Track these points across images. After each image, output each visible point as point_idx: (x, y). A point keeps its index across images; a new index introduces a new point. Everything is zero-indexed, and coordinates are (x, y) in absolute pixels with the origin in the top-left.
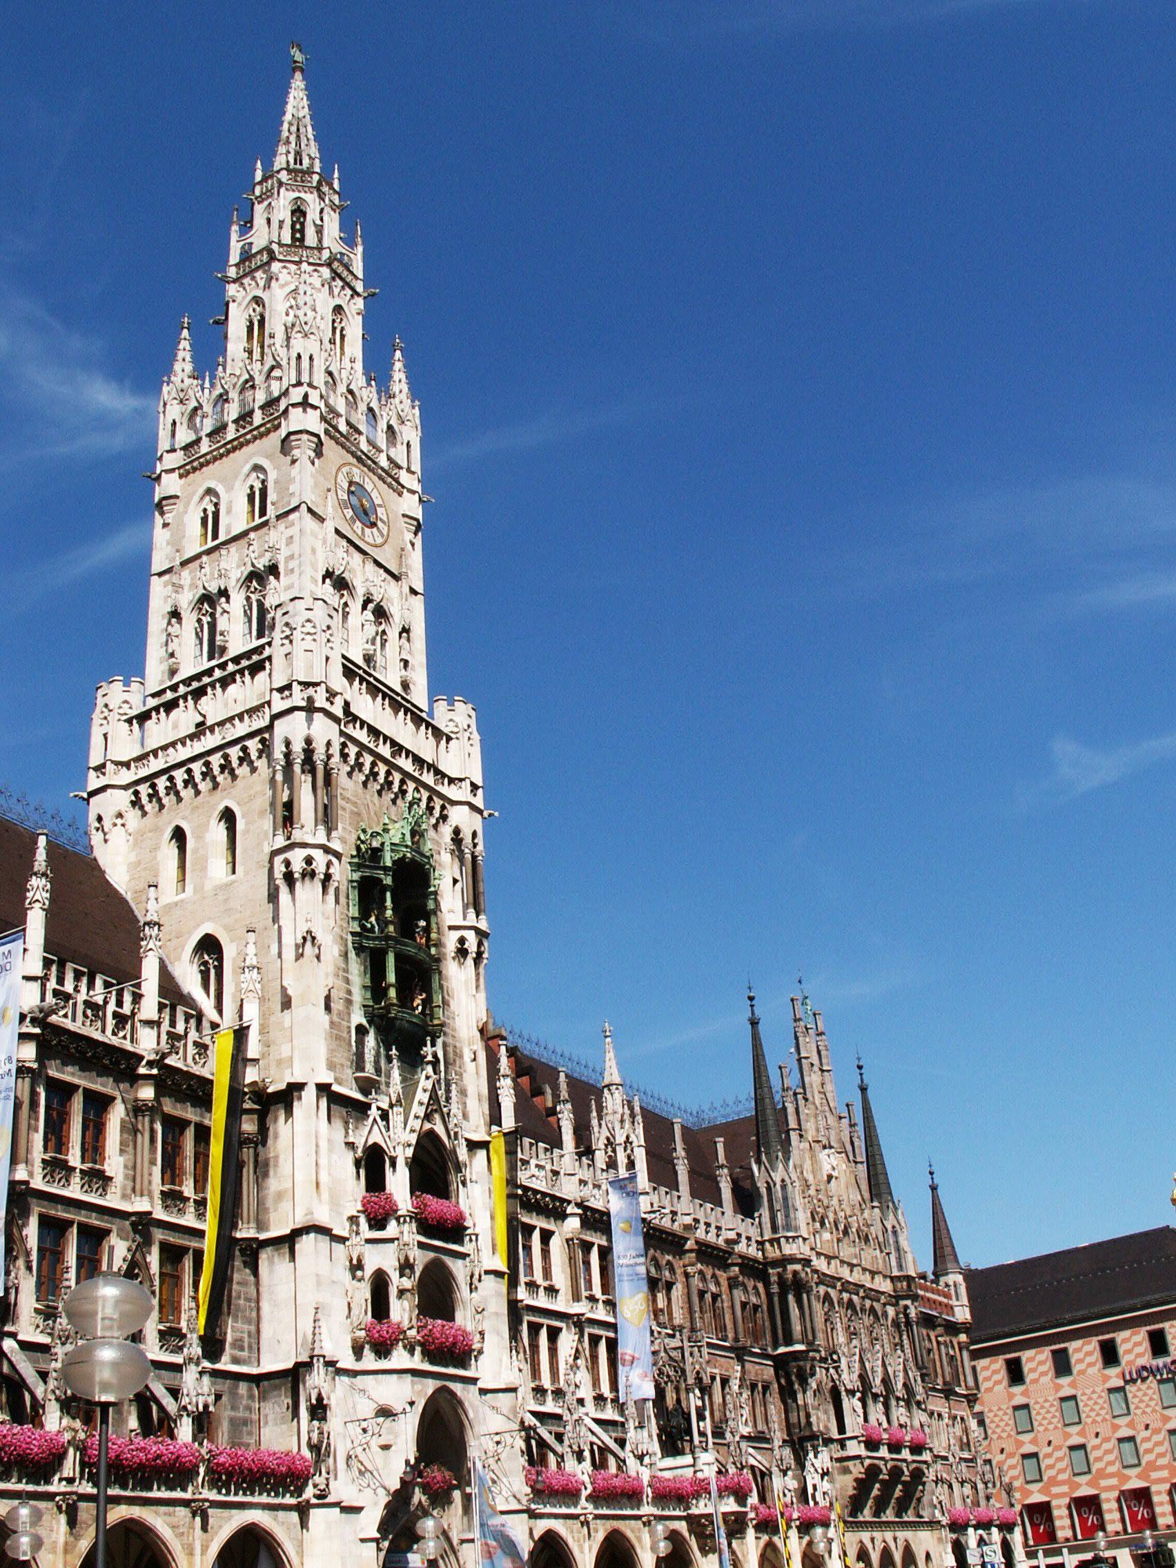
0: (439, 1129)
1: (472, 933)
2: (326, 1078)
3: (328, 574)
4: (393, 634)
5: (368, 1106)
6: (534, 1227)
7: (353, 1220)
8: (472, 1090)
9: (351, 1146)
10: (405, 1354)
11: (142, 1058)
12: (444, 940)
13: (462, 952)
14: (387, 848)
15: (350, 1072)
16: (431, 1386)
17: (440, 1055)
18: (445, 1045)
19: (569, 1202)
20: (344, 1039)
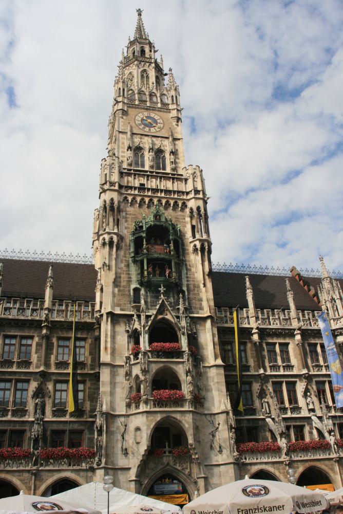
0: (169, 317)
1: (198, 241)
2: (109, 310)
3: (129, 148)
4: (167, 155)
5: (133, 315)
6: (276, 343)
7: (128, 358)
8: (204, 298)
9: (128, 331)
10: (144, 405)
11: (43, 321)
12: (187, 248)
13: (195, 250)
14: (144, 224)
15: (129, 305)
16: (159, 417)
17: (185, 288)
18: (188, 286)
19: (295, 330)
20: (126, 295)
